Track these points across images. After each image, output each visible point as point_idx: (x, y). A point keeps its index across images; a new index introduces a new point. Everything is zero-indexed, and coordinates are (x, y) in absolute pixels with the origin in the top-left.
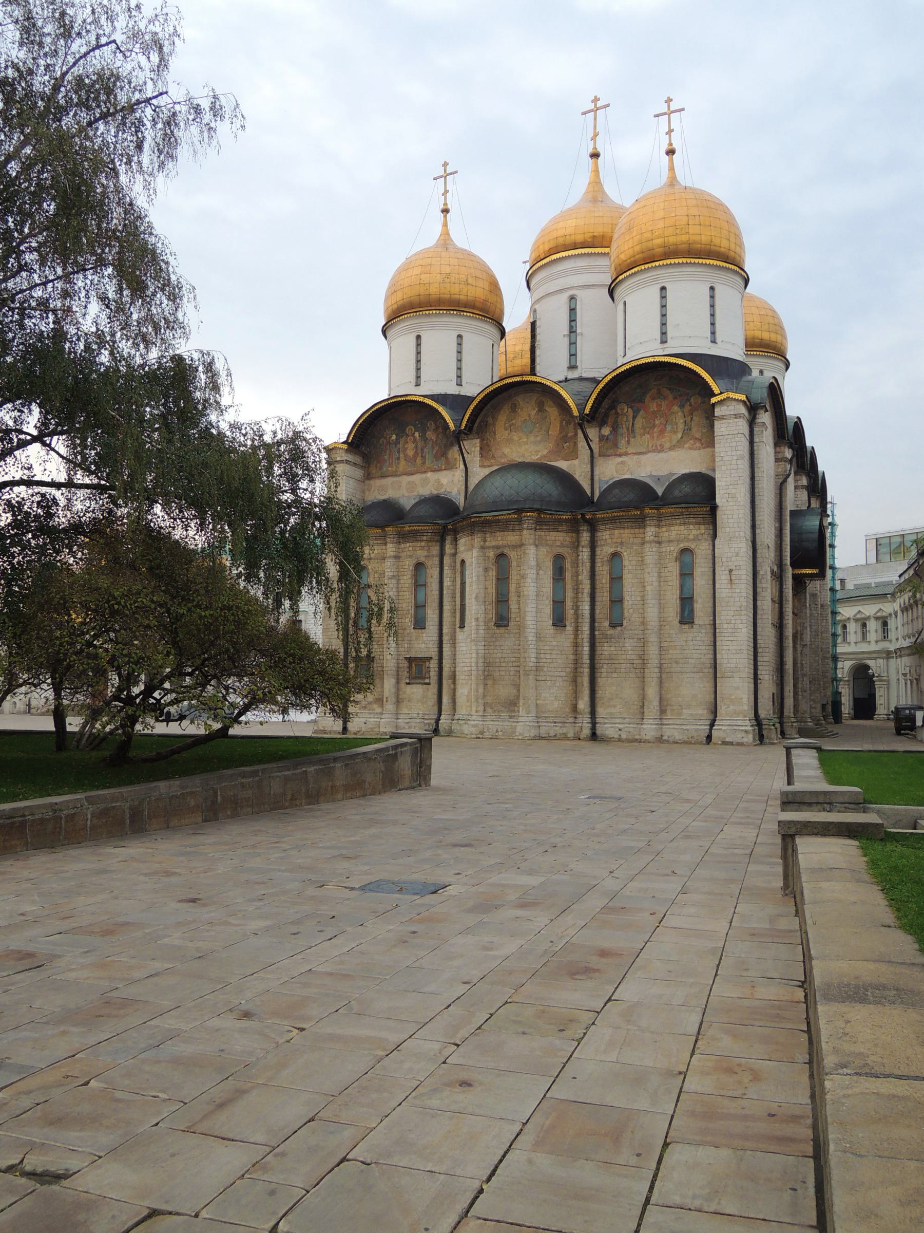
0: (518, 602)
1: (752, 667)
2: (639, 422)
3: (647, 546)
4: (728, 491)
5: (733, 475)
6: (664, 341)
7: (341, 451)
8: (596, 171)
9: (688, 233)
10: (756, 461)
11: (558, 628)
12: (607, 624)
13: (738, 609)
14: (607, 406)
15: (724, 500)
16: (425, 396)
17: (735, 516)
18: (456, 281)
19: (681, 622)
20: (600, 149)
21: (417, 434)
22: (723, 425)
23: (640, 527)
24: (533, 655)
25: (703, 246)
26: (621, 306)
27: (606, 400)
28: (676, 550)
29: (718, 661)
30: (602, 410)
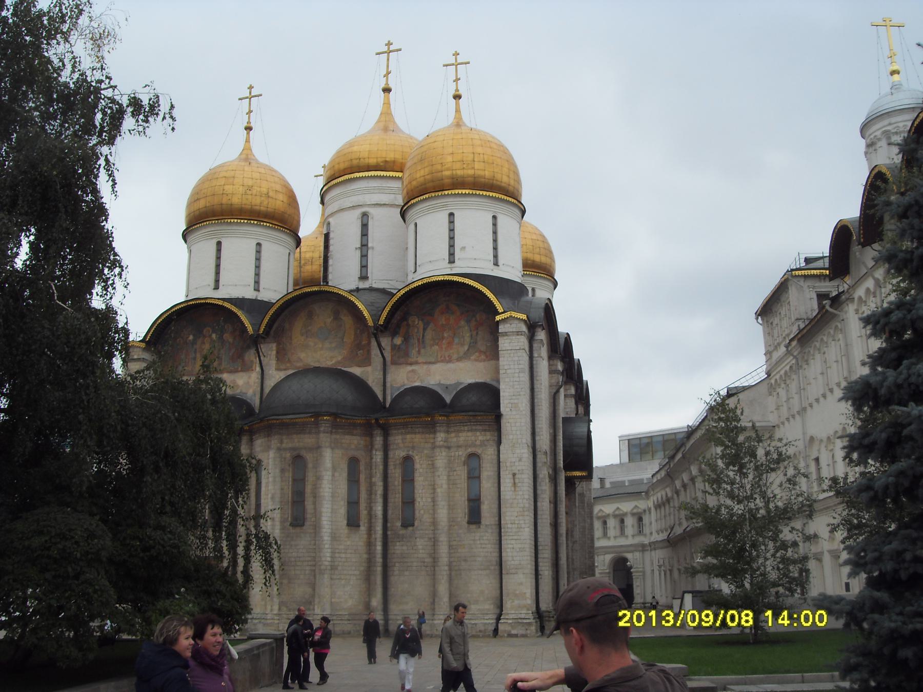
0: (314, 503)
1: (534, 563)
2: (429, 334)
3: (437, 450)
4: (512, 401)
5: (516, 387)
6: (452, 261)
7: (138, 349)
8: (387, 104)
9: (473, 168)
10: (535, 374)
11: (352, 528)
12: (399, 524)
13: (521, 510)
14: (399, 318)
15: (508, 409)
16: (224, 300)
17: (518, 424)
18: (258, 194)
19: (469, 523)
20: (391, 85)
21: (214, 336)
22: (506, 341)
23: (430, 433)
24: (328, 555)
25: (487, 180)
26: (412, 227)
27: (399, 313)
28: (464, 455)
29: (503, 559)
30: (394, 321)
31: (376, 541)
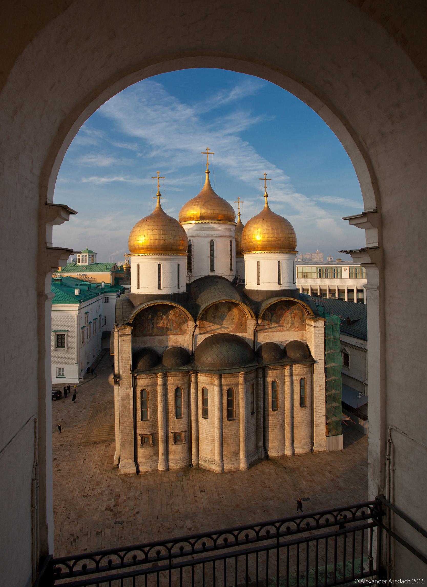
4: (319, 356)
5: (320, 349)
17: (321, 365)
28: (299, 379)
31: (261, 418)
